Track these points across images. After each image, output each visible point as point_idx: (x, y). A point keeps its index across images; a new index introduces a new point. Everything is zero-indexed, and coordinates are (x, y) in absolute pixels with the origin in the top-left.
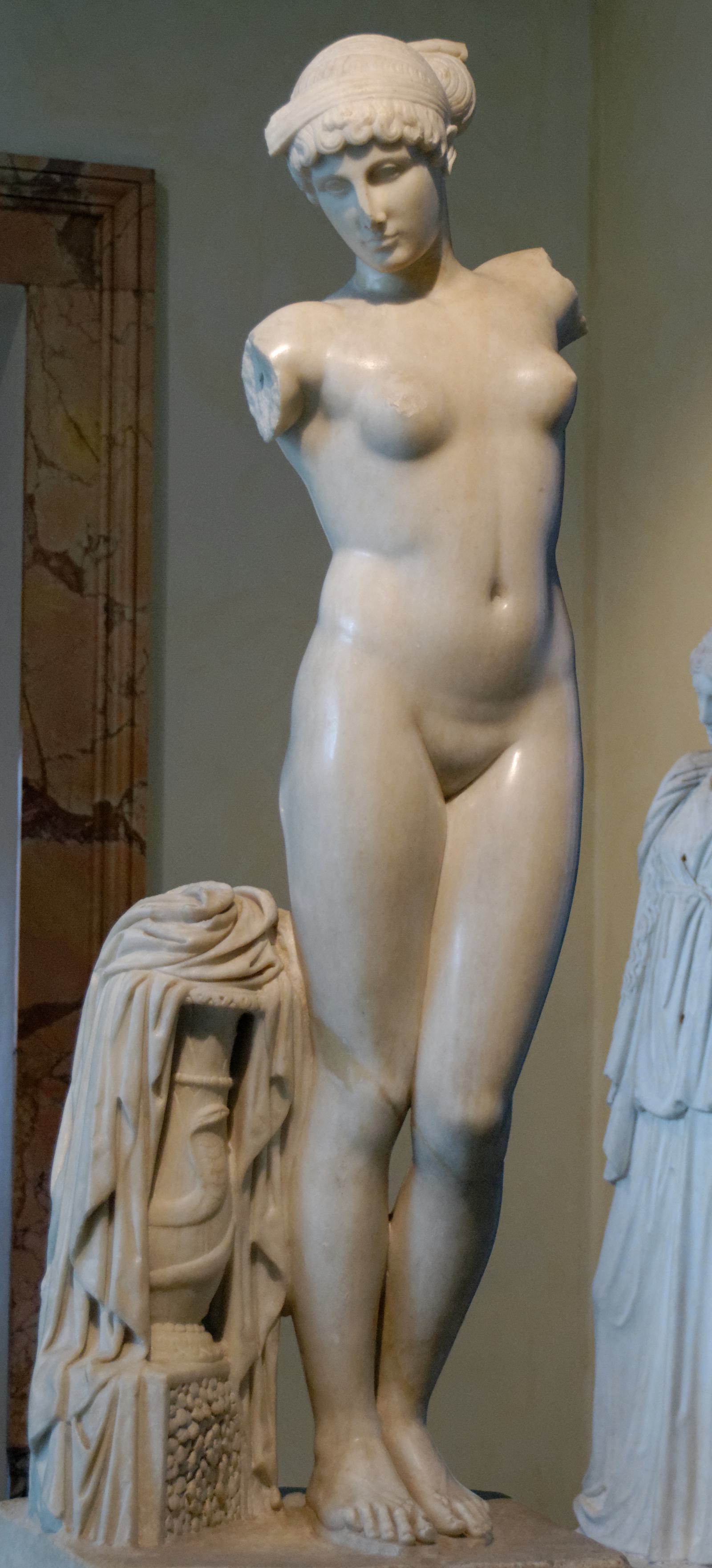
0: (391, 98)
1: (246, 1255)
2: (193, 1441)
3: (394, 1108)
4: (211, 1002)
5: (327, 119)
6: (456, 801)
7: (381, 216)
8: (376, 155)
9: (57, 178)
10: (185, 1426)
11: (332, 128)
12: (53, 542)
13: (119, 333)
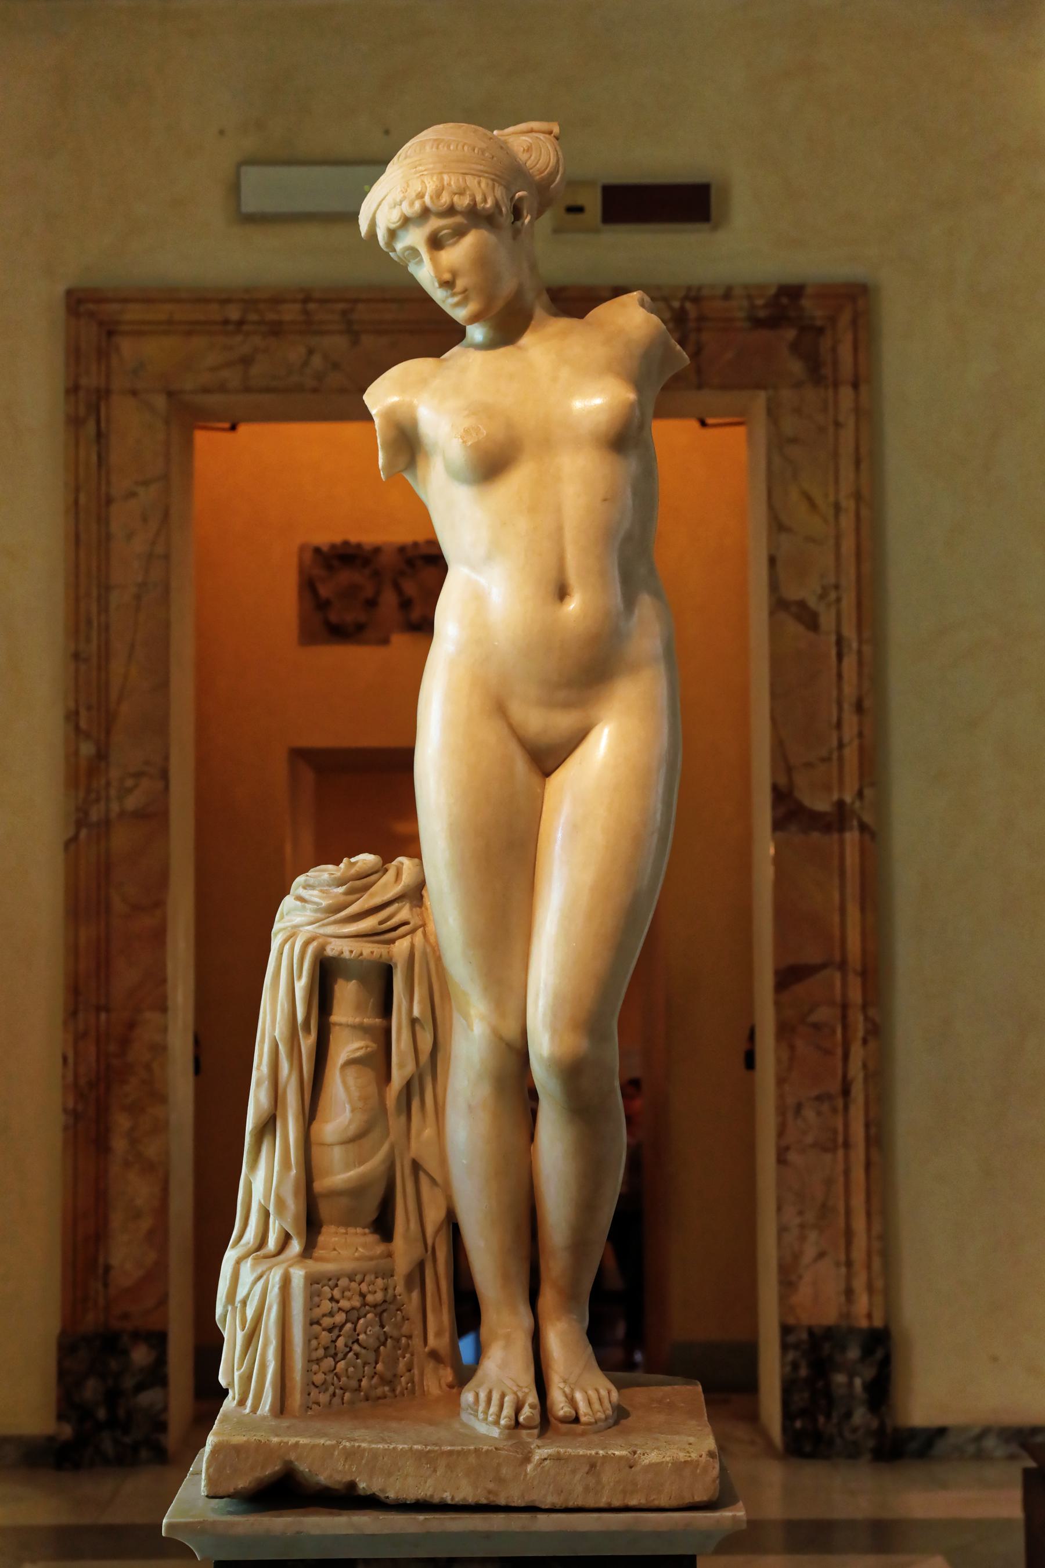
0: (441, 173)
1: (408, 1170)
3: (509, 1046)
5: (389, 200)
6: (553, 776)
7: (447, 276)
8: (434, 223)
9: (785, 301)
10: (331, 1314)
12: (792, 593)
13: (841, 419)
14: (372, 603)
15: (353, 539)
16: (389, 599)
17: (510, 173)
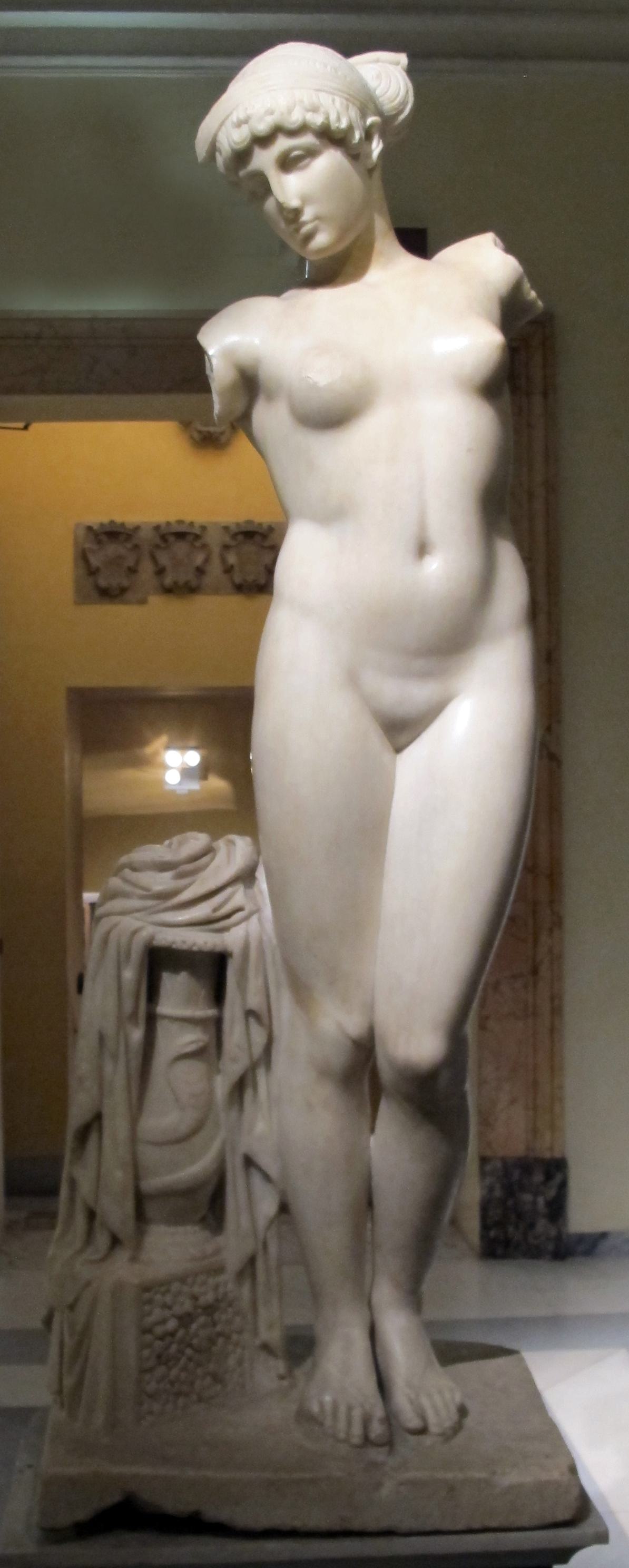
2: (172, 1334)
4: (174, 946)
5: (234, 118)
7: (294, 203)
10: (164, 1322)
11: (239, 124)
14: (132, 571)
15: (118, 519)
16: (147, 568)
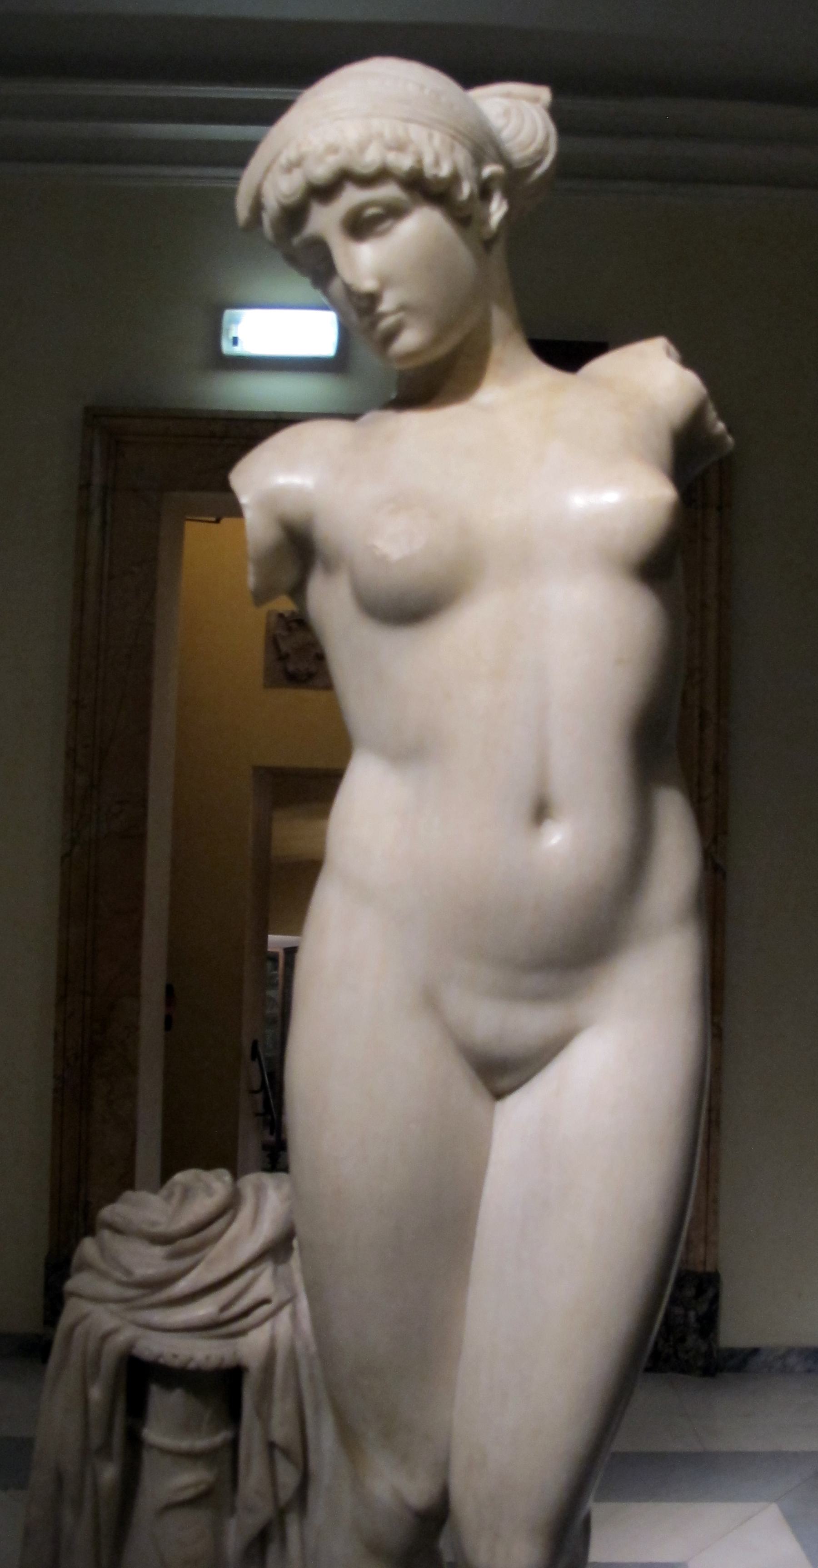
4: (161, 1361)
5: (283, 160)
17: (483, 145)
